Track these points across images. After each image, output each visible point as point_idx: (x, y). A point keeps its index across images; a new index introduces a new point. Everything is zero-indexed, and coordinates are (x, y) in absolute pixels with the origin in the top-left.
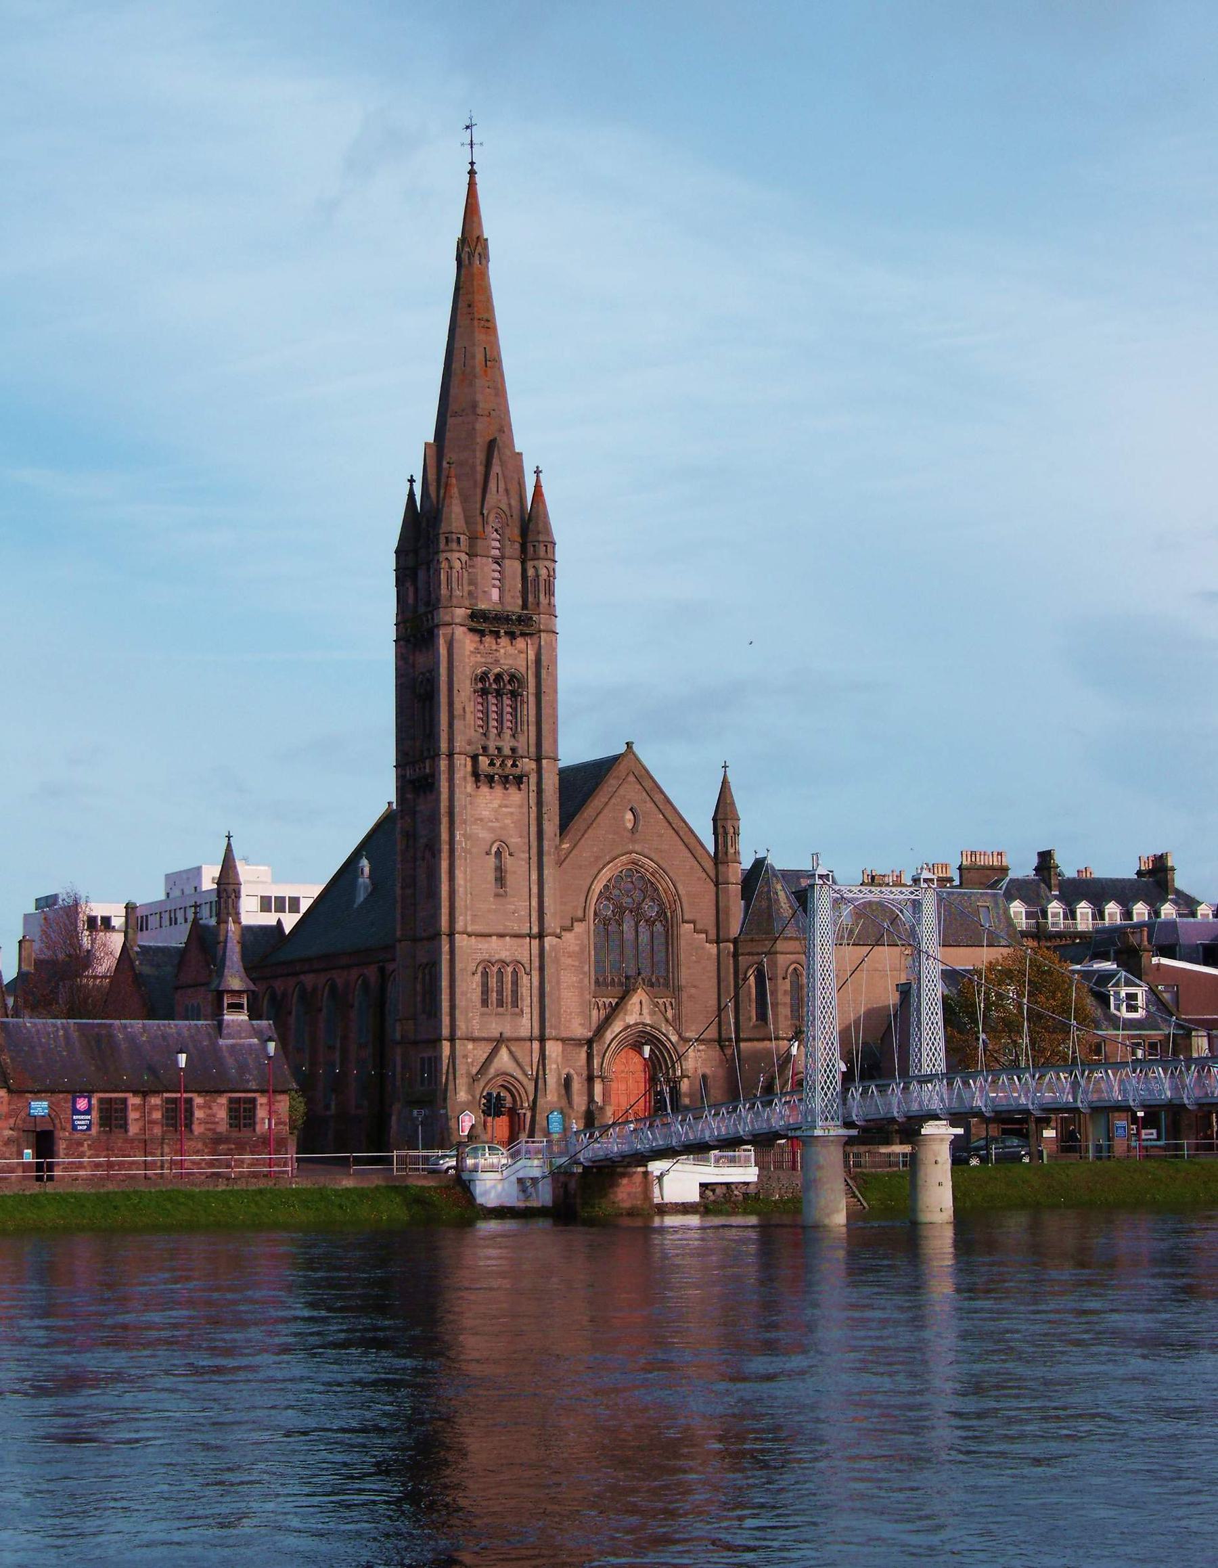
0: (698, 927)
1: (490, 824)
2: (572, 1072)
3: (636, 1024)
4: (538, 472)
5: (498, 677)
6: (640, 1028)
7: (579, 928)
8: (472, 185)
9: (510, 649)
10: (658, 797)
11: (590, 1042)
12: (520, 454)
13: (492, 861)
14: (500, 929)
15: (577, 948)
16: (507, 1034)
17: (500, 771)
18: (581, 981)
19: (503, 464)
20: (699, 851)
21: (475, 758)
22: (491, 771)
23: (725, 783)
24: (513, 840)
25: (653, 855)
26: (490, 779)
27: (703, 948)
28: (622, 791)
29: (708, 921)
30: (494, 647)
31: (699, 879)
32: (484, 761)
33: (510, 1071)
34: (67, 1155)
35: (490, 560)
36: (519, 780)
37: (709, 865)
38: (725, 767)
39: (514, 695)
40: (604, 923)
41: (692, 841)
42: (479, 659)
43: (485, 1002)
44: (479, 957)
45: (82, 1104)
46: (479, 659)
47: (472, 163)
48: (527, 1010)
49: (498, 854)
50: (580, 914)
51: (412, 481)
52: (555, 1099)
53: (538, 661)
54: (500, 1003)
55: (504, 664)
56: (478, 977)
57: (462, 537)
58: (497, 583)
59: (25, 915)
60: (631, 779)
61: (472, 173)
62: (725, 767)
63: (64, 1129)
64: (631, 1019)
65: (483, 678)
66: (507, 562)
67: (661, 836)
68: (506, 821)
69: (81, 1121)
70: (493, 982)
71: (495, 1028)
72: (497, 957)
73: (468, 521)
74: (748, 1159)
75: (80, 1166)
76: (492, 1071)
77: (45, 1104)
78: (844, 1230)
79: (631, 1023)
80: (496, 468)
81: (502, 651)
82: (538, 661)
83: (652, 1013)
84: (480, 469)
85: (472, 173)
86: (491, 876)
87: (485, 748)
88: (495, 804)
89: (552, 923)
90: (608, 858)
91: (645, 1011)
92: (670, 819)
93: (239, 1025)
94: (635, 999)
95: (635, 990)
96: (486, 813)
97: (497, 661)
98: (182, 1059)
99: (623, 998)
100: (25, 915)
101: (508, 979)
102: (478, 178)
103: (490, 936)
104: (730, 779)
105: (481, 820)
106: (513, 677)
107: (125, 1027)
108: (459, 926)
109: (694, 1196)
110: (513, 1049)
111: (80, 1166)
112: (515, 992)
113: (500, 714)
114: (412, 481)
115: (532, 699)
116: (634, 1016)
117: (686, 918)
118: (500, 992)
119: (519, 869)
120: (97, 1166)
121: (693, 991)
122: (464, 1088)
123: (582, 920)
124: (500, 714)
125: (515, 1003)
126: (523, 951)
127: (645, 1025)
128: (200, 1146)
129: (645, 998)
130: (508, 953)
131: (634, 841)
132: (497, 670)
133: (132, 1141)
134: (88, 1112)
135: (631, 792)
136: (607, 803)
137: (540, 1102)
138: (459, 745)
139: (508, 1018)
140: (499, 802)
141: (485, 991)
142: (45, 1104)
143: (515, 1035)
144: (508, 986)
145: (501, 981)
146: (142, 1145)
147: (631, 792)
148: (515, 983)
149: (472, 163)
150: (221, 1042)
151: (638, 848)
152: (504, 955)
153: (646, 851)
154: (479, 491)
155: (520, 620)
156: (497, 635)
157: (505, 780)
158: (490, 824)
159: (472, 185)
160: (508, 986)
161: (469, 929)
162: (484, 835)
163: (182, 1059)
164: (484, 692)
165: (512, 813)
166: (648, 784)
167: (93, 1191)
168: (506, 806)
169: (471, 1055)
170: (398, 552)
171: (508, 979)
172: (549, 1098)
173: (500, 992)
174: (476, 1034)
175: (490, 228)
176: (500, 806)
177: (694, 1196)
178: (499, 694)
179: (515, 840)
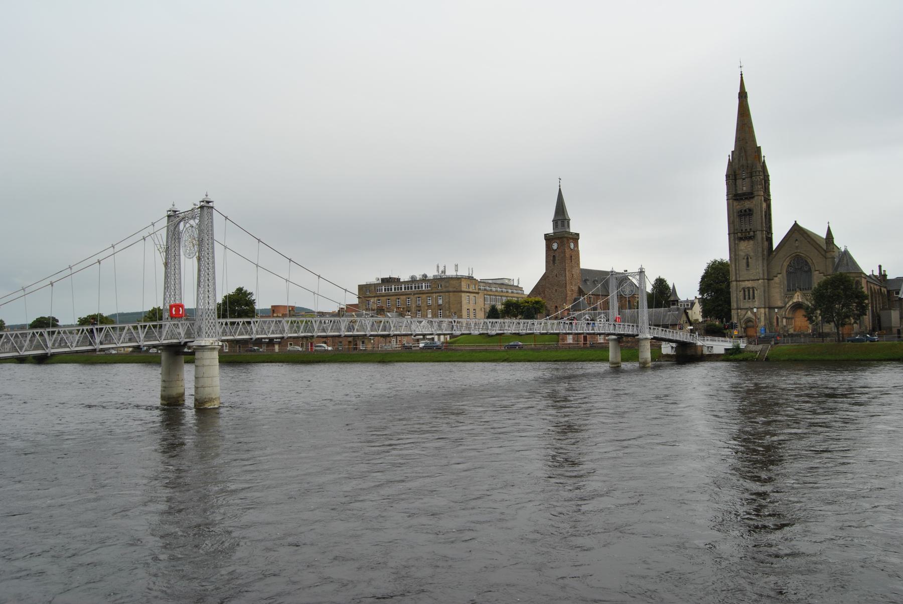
0: (821, 272)
3: (796, 302)
5: (745, 211)
7: (779, 276)
8: (742, 77)
9: (749, 203)
14: (748, 279)
15: (779, 282)
18: (780, 291)
23: (829, 228)
28: (793, 236)
42: (739, 207)
43: (745, 299)
44: (742, 287)
46: (739, 207)
49: (748, 258)
54: (749, 299)
61: (741, 74)
64: (795, 300)
65: (741, 211)
71: (747, 306)
72: (747, 286)
83: (802, 298)
85: (741, 74)
88: (746, 245)
90: (788, 255)
91: (799, 298)
94: (796, 295)
96: (743, 248)
97: (744, 206)
102: (743, 76)
103: (745, 281)
104: (830, 226)
106: (750, 210)
109: (723, 352)
117: (817, 269)
118: (749, 295)
123: (780, 274)
129: (799, 294)
141: (745, 296)
145: (749, 293)
148: (754, 293)
151: (799, 251)
152: (750, 285)
159: (742, 77)
173: (749, 295)
174: (742, 307)
177: (723, 352)
179: (752, 254)
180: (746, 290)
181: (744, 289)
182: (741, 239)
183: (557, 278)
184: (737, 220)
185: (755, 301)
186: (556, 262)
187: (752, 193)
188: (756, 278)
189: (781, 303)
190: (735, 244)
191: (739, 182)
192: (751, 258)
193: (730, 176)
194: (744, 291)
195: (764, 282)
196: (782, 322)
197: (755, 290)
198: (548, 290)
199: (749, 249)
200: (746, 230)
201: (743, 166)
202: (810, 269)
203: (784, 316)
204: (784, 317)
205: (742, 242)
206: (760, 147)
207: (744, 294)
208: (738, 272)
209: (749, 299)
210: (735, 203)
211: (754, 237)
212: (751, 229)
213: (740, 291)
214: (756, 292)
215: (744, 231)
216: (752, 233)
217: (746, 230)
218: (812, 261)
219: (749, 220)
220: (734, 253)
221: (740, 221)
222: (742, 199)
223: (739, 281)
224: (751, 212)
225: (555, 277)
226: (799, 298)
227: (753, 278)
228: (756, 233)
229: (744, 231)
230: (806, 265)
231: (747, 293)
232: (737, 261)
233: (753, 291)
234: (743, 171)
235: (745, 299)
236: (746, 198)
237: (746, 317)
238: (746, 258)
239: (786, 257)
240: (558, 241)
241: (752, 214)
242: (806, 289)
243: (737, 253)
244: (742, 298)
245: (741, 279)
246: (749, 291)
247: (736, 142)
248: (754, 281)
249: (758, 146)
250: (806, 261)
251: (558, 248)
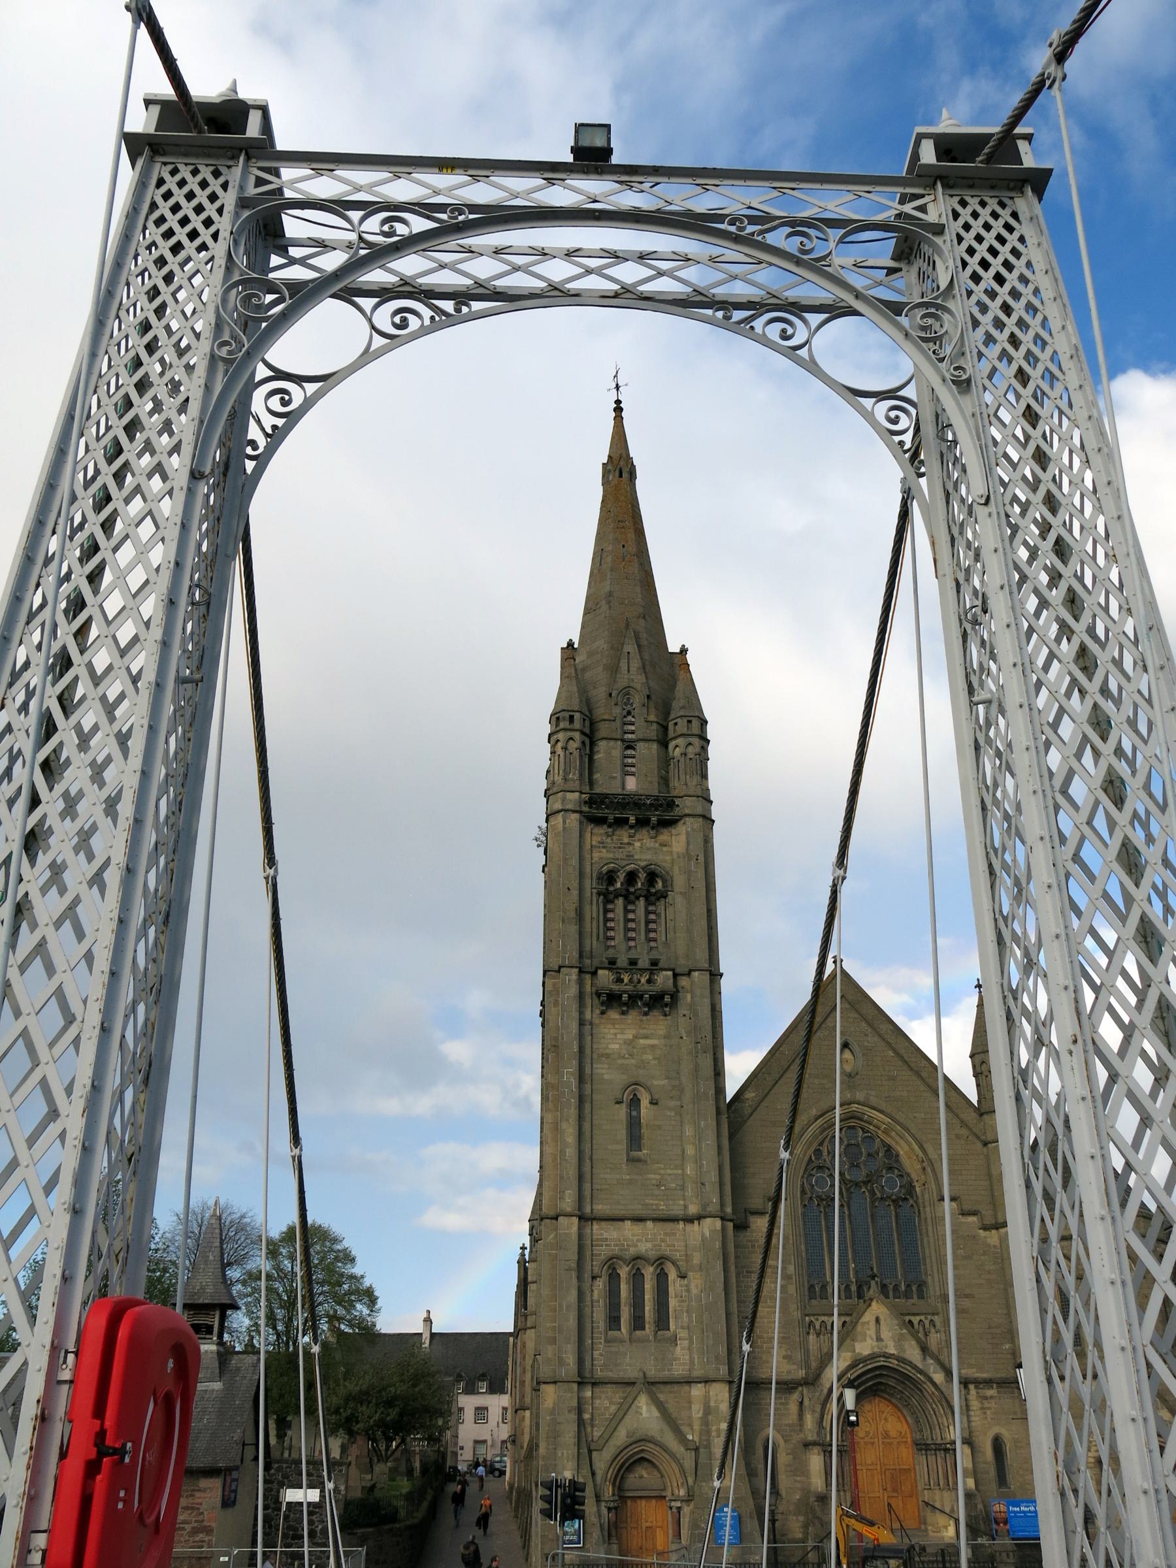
0: (966, 1207)
1: (620, 1061)
3: (873, 1357)
5: (631, 877)
9: (649, 843)
10: (884, 1027)
13: (622, 1111)
14: (637, 1209)
16: (652, 1373)
24: (655, 1083)
25: (883, 1106)
27: (975, 1237)
30: (626, 840)
43: (614, 1321)
44: (603, 1252)
46: (604, 854)
49: (635, 1102)
54: (638, 1322)
55: (640, 860)
56: (600, 1284)
61: (618, 409)
62: (979, 986)
64: (864, 1348)
65: (610, 877)
67: (893, 1078)
68: (645, 1057)
72: (632, 1251)
79: (866, 1352)
81: (637, 844)
83: (899, 1340)
85: (618, 409)
88: (629, 1035)
91: (886, 1334)
94: (869, 1317)
97: (630, 856)
103: (622, 1220)
105: (608, 1056)
106: (652, 877)
110: (661, 1397)
116: (869, 1341)
125: (662, 1322)
127: (887, 1356)
130: (649, 1245)
140: (634, 1032)
144: (649, 1297)
151: (860, 1096)
152: (644, 1248)
153: (874, 1101)
155: (655, 806)
158: (620, 1061)
160: (649, 1297)
164: (607, 897)
165: (653, 1046)
168: (646, 1037)
176: (636, 1037)
178: (627, 896)
180: (624, 1272)
181: (612, 1264)
182: (611, 1000)
184: (593, 910)
185: (674, 1340)
187: (671, 805)
188: (677, 1210)
190: (582, 1023)
191: (607, 752)
192: (654, 1103)
193: (577, 716)
194: (614, 1277)
195: (724, 1229)
196: (800, 1469)
197: (672, 1275)
200: (633, 962)
201: (626, 692)
202: (910, 1188)
203: (811, 1437)
204: (807, 1445)
205: (614, 1014)
208: (587, 1168)
209: (638, 1322)
210: (596, 835)
211: (674, 996)
212: (654, 963)
213: (594, 1278)
214: (675, 1285)
215: (622, 962)
216: (663, 979)
217: (633, 962)
218: (921, 1147)
219: (648, 922)
220: (575, 1063)
221: (606, 920)
222: (621, 822)
223: (594, 1219)
224: (660, 885)
227: (663, 1208)
228: (684, 982)
229: (622, 962)
230: (890, 1169)
231: (624, 1290)
232: (587, 1106)
233: (662, 1277)
234: (629, 713)
235: (614, 1321)
236: (643, 823)
237: (621, 1437)
238: (627, 1097)
241: (663, 895)
242: (896, 1288)
243: (588, 1070)
244: (599, 1315)
245: (601, 1208)
246: (637, 1278)
247: (587, 611)
248: (669, 1226)
249: (673, 647)
250: (889, 1149)
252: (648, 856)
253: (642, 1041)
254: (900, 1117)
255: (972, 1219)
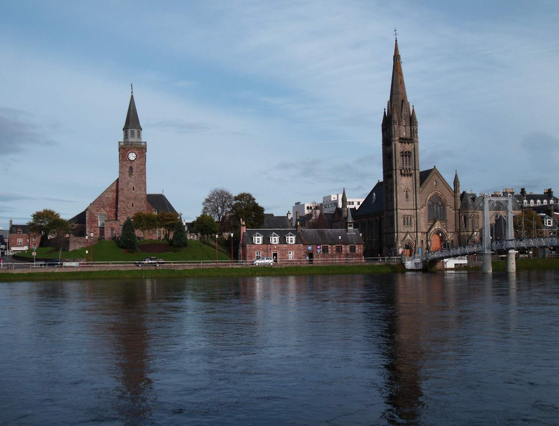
0: (451, 207)
2: (423, 239)
4: (413, 106)
5: (406, 152)
6: (438, 229)
7: (424, 207)
8: (396, 43)
10: (441, 178)
11: (427, 233)
12: (409, 102)
14: (407, 208)
15: (424, 212)
16: (409, 231)
17: (406, 173)
19: (405, 105)
20: (451, 190)
21: (401, 170)
22: (405, 173)
25: (441, 191)
26: (404, 175)
28: (433, 177)
29: (453, 205)
30: (405, 146)
31: (451, 196)
32: (403, 171)
33: (410, 240)
34: (316, 258)
35: (403, 126)
36: (411, 175)
37: (453, 193)
38: (456, 171)
39: (409, 156)
40: (429, 206)
41: (449, 188)
43: (404, 224)
44: (403, 214)
45: (319, 247)
47: (396, 39)
48: (413, 226)
50: (425, 204)
51: (385, 109)
52: (420, 245)
53: (414, 148)
54: (407, 224)
57: (397, 122)
58: (405, 131)
59: (293, 207)
60: (435, 174)
61: (396, 41)
63: (315, 253)
64: (436, 228)
65: (402, 152)
66: (407, 127)
69: (319, 251)
70: (406, 220)
71: (406, 230)
73: (398, 118)
74: (465, 258)
75: (319, 260)
76: (406, 239)
77: (311, 247)
78: (491, 274)
80: (404, 106)
82: (414, 148)
83: (441, 226)
84: (400, 106)
85: (396, 41)
86: (405, 196)
87: (403, 168)
89: (419, 207)
91: (439, 226)
92: (444, 183)
93: (351, 230)
94: (437, 223)
95: (437, 221)
96: (404, 182)
97: (405, 149)
98: (340, 237)
99: (434, 223)
100: (293, 207)
101: (409, 219)
102: (398, 42)
106: (409, 152)
107: (327, 230)
108: (398, 207)
109: (453, 267)
110: (410, 234)
111: (319, 260)
112: (411, 222)
113: (406, 160)
114: (385, 109)
115: (413, 157)
117: (448, 205)
118: (407, 222)
119: (411, 195)
120: (322, 260)
121: (449, 221)
122: (400, 243)
123: (425, 206)
124: (406, 160)
126: (412, 213)
128: (344, 256)
129: (439, 223)
131: (436, 188)
132: (405, 151)
133: (329, 255)
134: (320, 249)
135: (435, 177)
136: (430, 180)
137: (417, 246)
138: (397, 168)
139: (409, 227)
141: (404, 222)
142: (311, 247)
143: (411, 231)
144: (409, 221)
146: (331, 256)
147: (435, 177)
148: (411, 220)
149: (396, 39)
150: (347, 233)
151: (437, 189)
152: (408, 214)
153: (439, 190)
154: (400, 111)
155: (410, 139)
156: (405, 143)
157: (408, 175)
159: (396, 43)
160: (409, 221)
161: (400, 208)
162: (403, 187)
163: (340, 237)
164: (403, 156)
165: (409, 183)
166: (439, 175)
167: (324, 266)
168: (408, 181)
169: (402, 236)
170: (382, 125)
171: (409, 219)
172: (418, 245)
173: (407, 222)
175: (401, 52)
176: (407, 181)
177: (453, 267)
178: (406, 156)
179: (410, 188)
183: (134, 192)
186: (133, 174)
189: (425, 229)
198: (122, 204)
199: (408, 184)
206: (409, 102)
207: (404, 220)
225: (132, 190)
226: (439, 226)
239: (429, 193)
240: (137, 152)
251: (136, 159)
252: (408, 149)
253: (408, 182)
254: (443, 193)
255: (452, 209)
